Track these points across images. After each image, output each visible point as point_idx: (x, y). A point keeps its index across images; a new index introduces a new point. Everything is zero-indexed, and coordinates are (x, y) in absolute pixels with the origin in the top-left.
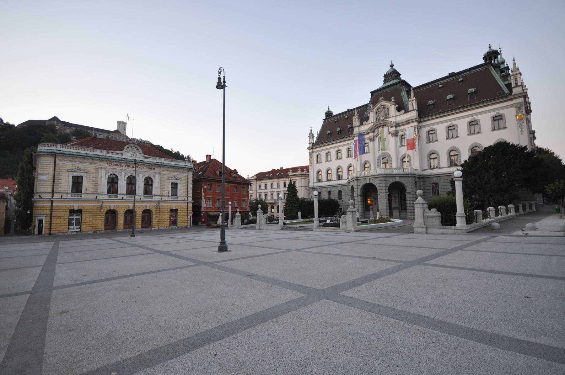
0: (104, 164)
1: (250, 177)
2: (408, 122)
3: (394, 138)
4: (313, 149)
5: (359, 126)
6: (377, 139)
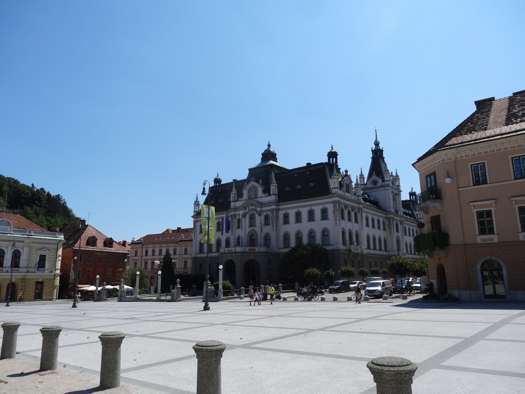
1: (135, 240)
2: (269, 204)
3: (259, 217)
4: (197, 218)
5: (235, 201)
6: (248, 216)
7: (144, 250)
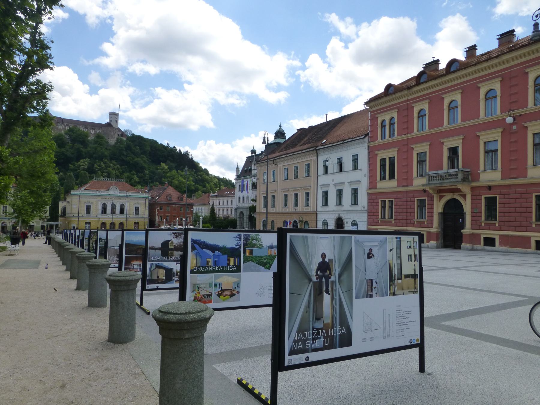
0: (100, 198)
7: (218, 201)
